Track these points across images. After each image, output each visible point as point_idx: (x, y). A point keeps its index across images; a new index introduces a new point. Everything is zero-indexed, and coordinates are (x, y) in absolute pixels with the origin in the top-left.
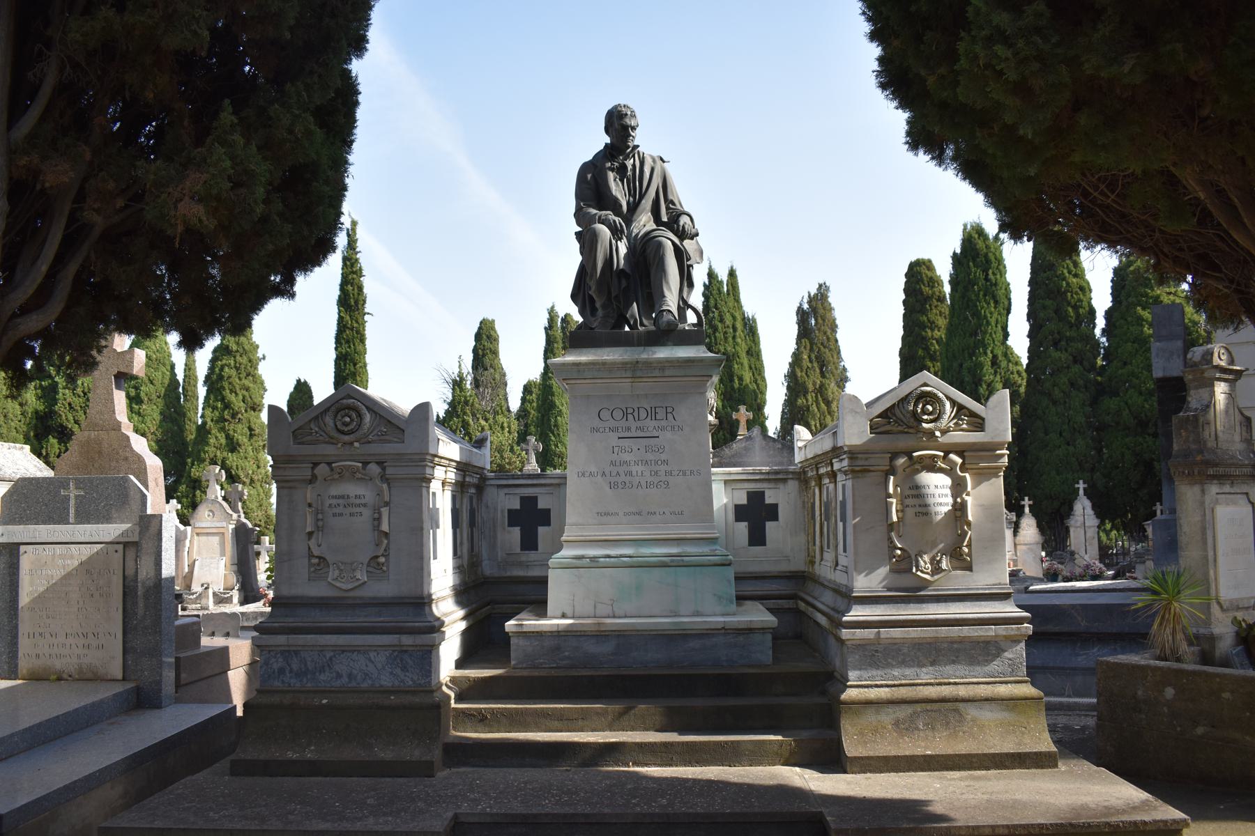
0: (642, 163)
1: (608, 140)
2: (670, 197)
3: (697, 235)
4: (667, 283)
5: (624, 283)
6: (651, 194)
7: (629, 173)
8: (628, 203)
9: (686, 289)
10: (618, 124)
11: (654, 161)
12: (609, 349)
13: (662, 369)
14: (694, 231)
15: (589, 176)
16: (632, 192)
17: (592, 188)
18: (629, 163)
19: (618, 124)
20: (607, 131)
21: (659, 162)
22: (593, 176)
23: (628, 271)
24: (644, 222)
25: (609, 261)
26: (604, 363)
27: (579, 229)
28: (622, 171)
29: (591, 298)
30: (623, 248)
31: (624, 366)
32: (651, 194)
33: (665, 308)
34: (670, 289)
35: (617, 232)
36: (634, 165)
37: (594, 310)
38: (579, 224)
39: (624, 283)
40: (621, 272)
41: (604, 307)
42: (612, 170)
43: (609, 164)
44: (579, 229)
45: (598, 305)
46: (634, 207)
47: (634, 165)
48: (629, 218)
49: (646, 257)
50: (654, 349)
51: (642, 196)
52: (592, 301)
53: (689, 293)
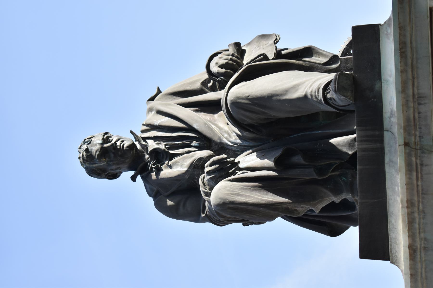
0: (153, 127)
1: (127, 175)
2: (197, 86)
3: (237, 45)
4: (287, 91)
5: (298, 159)
6: (188, 114)
7: (162, 146)
8: (200, 148)
9: (315, 59)
10: (106, 161)
11: (150, 110)
12: (389, 192)
13: (419, 99)
14: (231, 51)
15: (170, 203)
16: (185, 143)
17: (181, 199)
18: (152, 145)
19: (106, 161)
20: (114, 176)
21: (158, 104)
22: (169, 197)
23: (278, 153)
24: (222, 128)
25: (265, 183)
26: (410, 204)
28: (161, 157)
30: (248, 159)
31: (413, 169)
32: (188, 114)
33: (321, 96)
34: (295, 88)
35: (224, 170)
36: (155, 138)
39: (298, 159)
40: (279, 164)
41: (336, 191)
42: (159, 170)
43: (153, 175)
45: (337, 200)
46: (205, 142)
47: (155, 138)
48: (219, 147)
49: (264, 123)
50: (386, 115)
51: (190, 129)
52: (332, 206)
53: (320, 54)
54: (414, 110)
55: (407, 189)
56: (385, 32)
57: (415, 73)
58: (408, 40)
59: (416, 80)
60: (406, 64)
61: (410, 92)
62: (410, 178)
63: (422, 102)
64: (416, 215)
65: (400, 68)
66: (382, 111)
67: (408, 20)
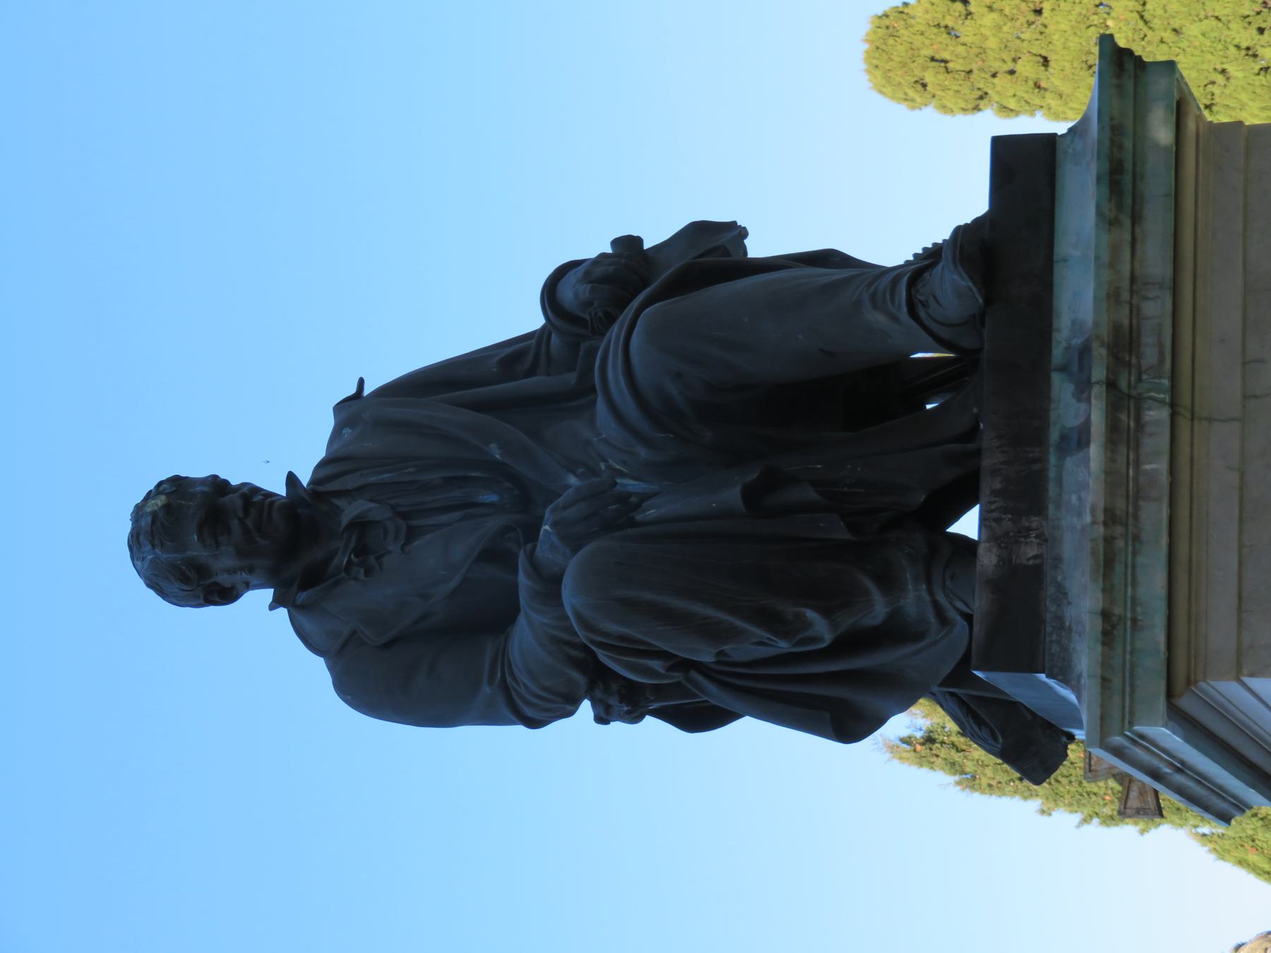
10: (200, 539)
19: (200, 539)
27: (586, 707)
29: (851, 643)
37: (895, 632)
38: (566, 707)
44: (586, 707)
54: (1131, 311)
55: (1106, 482)
56: (1070, 151)
57: (1137, 230)
58: (1128, 157)
59: (1138, 246)
60: (1120, 207)
61: (1126, 269)
62: (1113, 460)
63: (1150, 296)
64: (1120, 543)
65: (1107, 213)
66: (1050, 325)
67: (1131, 114)
